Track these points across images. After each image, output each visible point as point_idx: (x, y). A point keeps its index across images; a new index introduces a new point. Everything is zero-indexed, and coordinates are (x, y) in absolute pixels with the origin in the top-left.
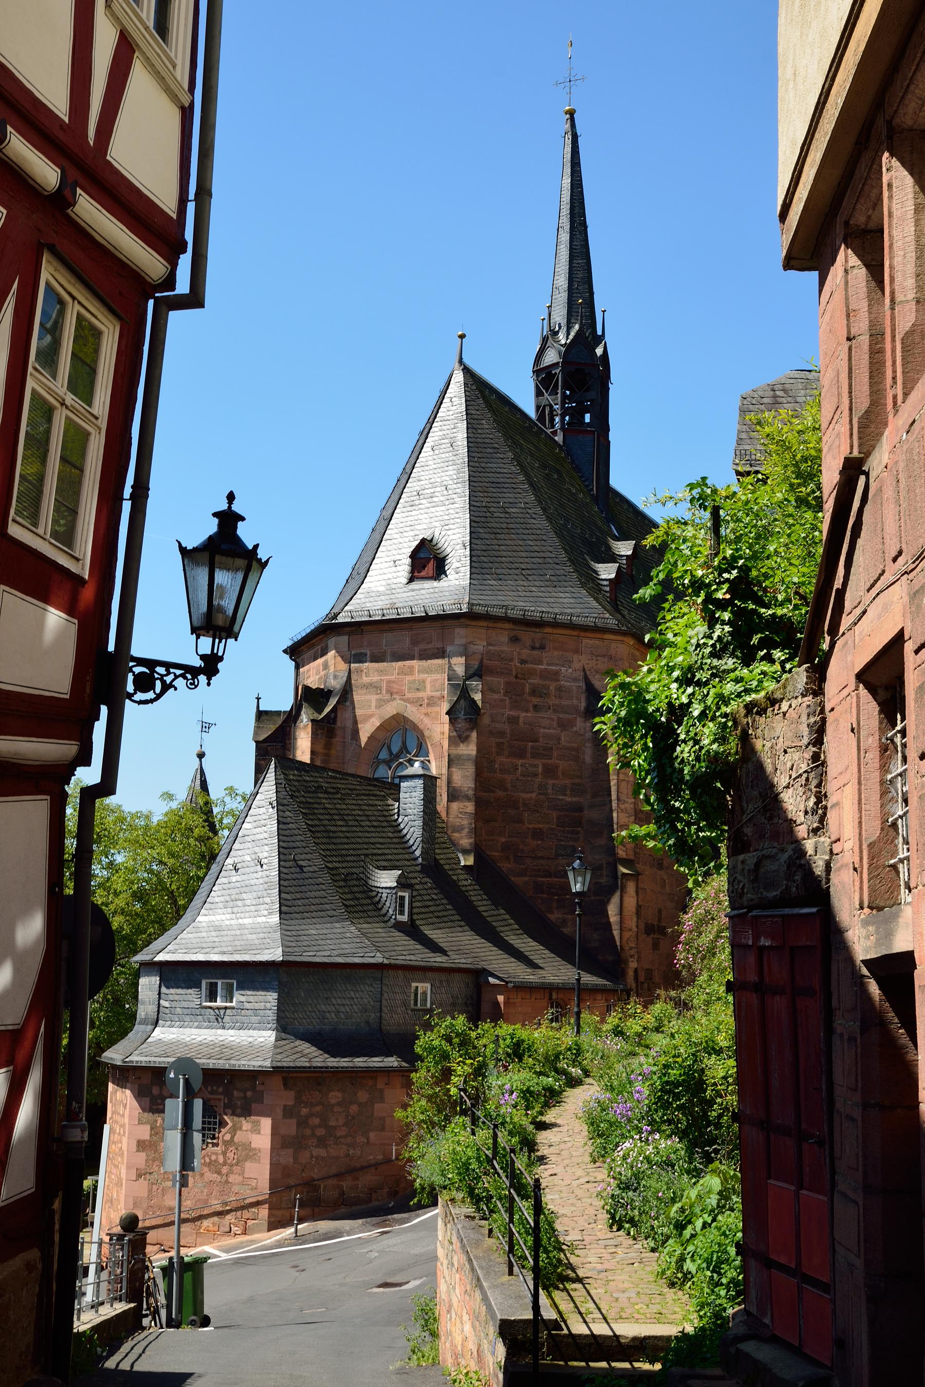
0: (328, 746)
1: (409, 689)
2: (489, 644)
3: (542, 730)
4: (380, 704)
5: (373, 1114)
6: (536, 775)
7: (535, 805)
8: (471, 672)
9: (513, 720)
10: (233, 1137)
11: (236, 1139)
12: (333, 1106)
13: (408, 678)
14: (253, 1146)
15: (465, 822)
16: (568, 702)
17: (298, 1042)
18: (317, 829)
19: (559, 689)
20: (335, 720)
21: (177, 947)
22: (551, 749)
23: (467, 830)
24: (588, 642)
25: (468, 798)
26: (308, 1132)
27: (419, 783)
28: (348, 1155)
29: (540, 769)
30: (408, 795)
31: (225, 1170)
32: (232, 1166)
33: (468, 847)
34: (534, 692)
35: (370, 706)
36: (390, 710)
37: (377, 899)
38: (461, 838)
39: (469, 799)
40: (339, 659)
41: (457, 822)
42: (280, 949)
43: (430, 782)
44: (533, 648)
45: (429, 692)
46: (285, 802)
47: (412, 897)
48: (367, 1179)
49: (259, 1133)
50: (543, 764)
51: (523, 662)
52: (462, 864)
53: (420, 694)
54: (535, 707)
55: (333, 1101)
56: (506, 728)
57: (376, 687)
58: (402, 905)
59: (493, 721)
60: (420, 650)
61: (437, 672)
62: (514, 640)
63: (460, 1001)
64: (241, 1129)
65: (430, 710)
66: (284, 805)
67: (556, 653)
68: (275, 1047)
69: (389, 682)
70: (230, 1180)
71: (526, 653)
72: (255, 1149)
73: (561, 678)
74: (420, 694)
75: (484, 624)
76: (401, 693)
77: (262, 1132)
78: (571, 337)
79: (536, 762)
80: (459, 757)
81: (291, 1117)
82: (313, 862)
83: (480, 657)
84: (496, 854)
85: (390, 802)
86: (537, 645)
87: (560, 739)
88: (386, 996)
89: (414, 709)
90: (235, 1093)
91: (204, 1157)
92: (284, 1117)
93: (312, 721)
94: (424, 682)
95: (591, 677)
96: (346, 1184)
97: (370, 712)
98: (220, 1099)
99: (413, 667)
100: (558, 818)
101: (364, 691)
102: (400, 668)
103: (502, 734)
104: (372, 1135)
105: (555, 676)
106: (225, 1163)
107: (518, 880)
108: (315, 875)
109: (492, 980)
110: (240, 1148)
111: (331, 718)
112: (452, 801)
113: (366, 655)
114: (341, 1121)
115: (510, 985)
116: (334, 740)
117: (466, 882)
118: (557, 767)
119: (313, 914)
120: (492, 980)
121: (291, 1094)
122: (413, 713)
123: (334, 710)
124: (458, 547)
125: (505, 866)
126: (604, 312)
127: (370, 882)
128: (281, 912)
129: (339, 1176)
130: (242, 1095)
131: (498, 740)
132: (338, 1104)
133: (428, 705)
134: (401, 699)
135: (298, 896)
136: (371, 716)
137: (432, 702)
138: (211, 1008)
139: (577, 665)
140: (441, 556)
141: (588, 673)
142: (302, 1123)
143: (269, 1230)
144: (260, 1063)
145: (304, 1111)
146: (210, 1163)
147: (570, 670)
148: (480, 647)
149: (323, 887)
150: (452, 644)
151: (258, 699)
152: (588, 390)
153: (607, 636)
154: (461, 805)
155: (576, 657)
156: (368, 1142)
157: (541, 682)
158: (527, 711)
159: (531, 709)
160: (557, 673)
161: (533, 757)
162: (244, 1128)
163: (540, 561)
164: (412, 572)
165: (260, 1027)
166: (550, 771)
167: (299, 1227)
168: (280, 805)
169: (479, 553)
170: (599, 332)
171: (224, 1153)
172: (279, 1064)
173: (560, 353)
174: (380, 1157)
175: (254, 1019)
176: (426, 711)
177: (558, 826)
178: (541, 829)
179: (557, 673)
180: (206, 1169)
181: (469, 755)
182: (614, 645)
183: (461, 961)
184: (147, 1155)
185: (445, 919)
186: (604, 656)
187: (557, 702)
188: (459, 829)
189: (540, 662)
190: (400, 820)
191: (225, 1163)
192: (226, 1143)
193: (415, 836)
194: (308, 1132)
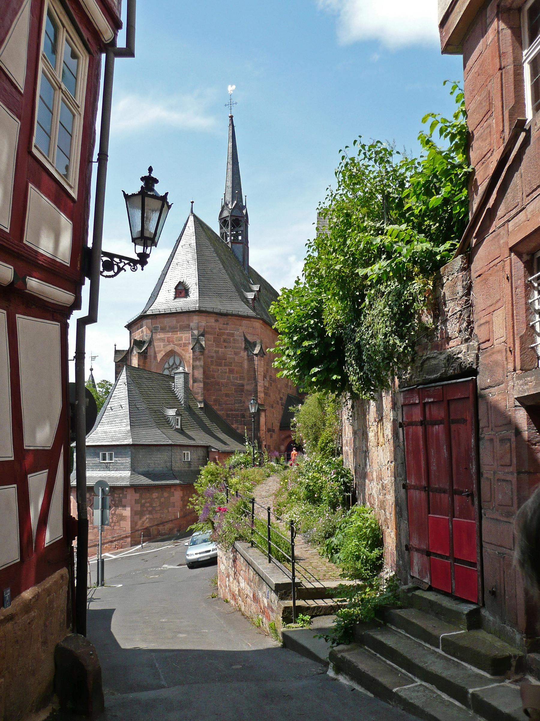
0: (145, 363)
4: (165, 346)
6: (226, 373)
8: (200, 333)
9: (217, 352)
10: (115, 512)
11: (116, 513)
12: (155, 499)
15: (200, 391)
16: (238, 345)
17: (140, 475)
18: (144, 393)
19: (234, 340)
20: (147, 353)
21: (89, 440)
22: (231, 363)
23: (200, 394)
24: (245, 322)
25: (200, 381)
26: (145, 509)
27: (182, 375)
28: (160, 517)
30: (178, 380)
31: (112, 525)
32: (115, 523)
33: (201, 400)
34: (225, 341)
35: (161, 347)
36: (169, 348)
37: (168, 420)
38: (198, 397)
39: (201, 382)
40: (147, 329)
41: (197, 391)
42: (131, 439)
43: (186, 374)
44: (224, 324)
46: (130, 383)
47: (181, 419)
48: (168, 526)
50: (229, 369)
51: (220, 329)
52: (199, 407)
53: (181, 342)
54: (225, 347)
55: (154, 497)
56: (214, 355)
58: (178, 422)
62: (217, 321)
63: (201, 458)
65: (184, 348)
66: (130, 384)
67: (232, 326)
68: (131, 477)
69: (169, 337)
71: (221, 325)
72: (124, 516)
73: (235, 336)
74: (181, 342)
75: (205, 314)
76: (173, 342)
78: (233, 206)
79: (226, 368)
80: (197, 366)
81: (138, 503)
82: (142, 406)
83: (203, 327)
85: (171, 383)
86: (226, 323)
87: (235, 359)
88: (173, 456)
89: (178, 348)
92: (135, 503)
93: (138, 353)
94: (182, 337)
96: (161, 528)
97: (161, 349)
100: (235, 389)
103: (212, 357)
104: (170, 509)
105: (232, 335)
107: (220, 413)
108: (143, 411)
109: (213, 450)
111: (145, 352)
114: (158, 504)
115: (220, 451)
116: (146, 360)
117: (201, 414)
118: (234, 369)
119: (143, 426)
120: (213, 450)
121: (138, 495)
122: (177, 349)
123: (146, 348)
124: (193, 285)
125: (215, 408)
126: (246, 196)
127: (165, 413)
128: (131, 425)
129: (158, 525)
131: (211, 359)
132: (157, 498)
135: (137, 419)
136: (161, 351)
137: (185, 345)
138: (104, 463)
139: (241, 331)
140: (187, 288)
142: (143, 506)
143: (131, 546)
144: (125, 484)
145: (143, 501)
148: (203, 324)
149: (147, 415)
150: (193, 322)
151: (115, 345)
152: (240, 227)
153: (252, 320)
154: (198, 384)
156: (168, 511)
157: (228, 337)
158: (222, 348)
160: (233, 334)
163: (226, 291)
164: (176, 295)
165: (124, 469)
167: (143, 545)
168: (129, 384)
169: (202, 287)
170: (244, 205)
172: (133, 484)
173: (229, 212)
174: (173, 517)
175: (122, 467)
176: (183, 349)
178: (228, 393)
179: (233, 334)
182: (255, 323)
183: (201, 443)
185: (194, 427)
186: (251, 327)
190: (175, 390)
191: (112, 522)
193: (181, 396)
194: (145, 509)
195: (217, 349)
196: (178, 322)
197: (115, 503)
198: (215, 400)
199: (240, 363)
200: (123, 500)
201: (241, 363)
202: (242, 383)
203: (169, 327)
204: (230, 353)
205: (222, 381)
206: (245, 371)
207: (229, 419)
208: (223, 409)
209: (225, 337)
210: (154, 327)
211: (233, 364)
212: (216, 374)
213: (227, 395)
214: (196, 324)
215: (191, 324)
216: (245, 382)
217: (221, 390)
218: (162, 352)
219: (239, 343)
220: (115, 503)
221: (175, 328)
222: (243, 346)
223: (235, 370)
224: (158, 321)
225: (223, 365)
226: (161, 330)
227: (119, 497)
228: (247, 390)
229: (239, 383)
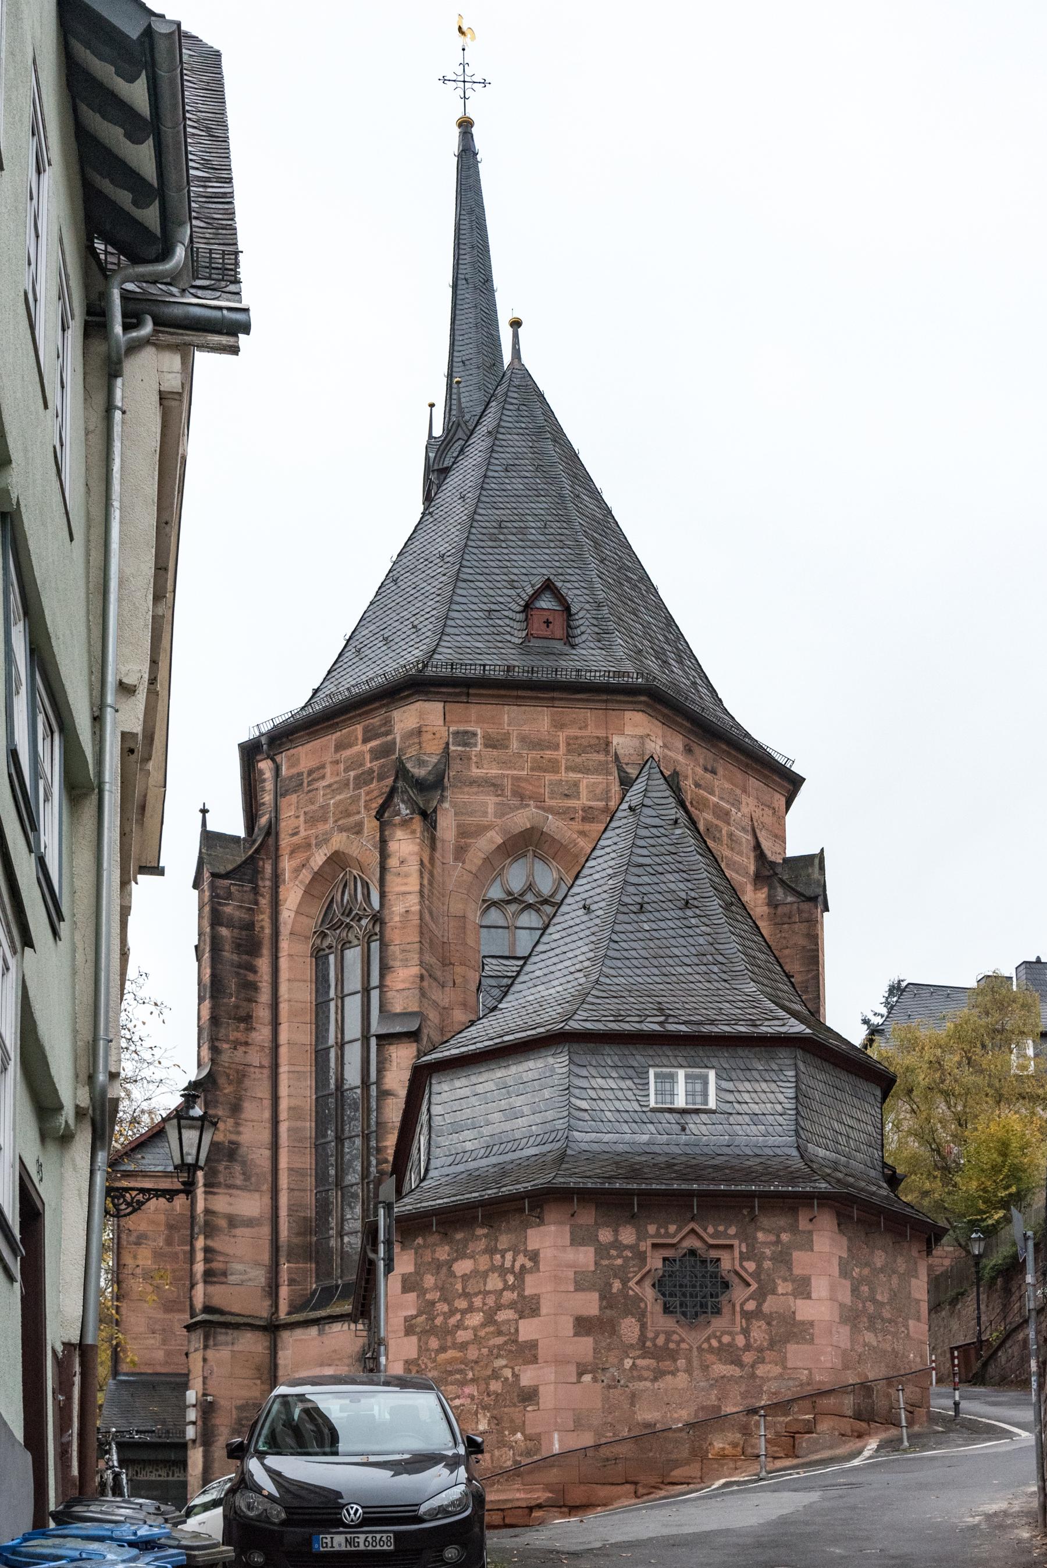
1: (552, 792)
2: (665, 746)
4: (502, 811)
10: (760, 1305)
11: (766, 1308)
13: (549, 777)
14: (798, 1318)
19: (731, 835)
31: (748, 1358)
32: (760, 1350)
36: (522, 819)
45: (584, 800)
49: (809, 1297)
57: (494, 785)
60: (568, 737)
61: (596, 771)
64: (774, 1292)
65: (587, 827)
69: (517, 779)
70: (759, 1373)
71: (699, 771)
72: (803, 1323)
73: (732, 822)
76: (539, 800)
77: (814, 1295)
89: (560, 824)
90: (760, 1236)
91: (708, 1340)
94: (576, 784)
95: (757, 831)
98: (731, 1247)
101: (475, 789)
102: (534, 760)
106: (748, 1347)
110: (774, 1323)
130: (772, 1238)
133: (584, 819)
134: (537, 807)
146: (719, 1349)
151: (204, 811)
162: (780, 1290)
171: (746, 1332)
180: (710, 1358)
184: (596, 1342)
191: (748, 1347)
192: (747, 1316)
197: (759, 1266)
200: (796, 1255)
203: (523, 739)
210: (457, 733)
214: (636, 742)
215: (616, 740)
218: (491, 834)
220: (759, 1266)
221: (549, 748)
222: (752, 868)
224: (474, 710)
226: (486, 746)
227: (778, 1241)
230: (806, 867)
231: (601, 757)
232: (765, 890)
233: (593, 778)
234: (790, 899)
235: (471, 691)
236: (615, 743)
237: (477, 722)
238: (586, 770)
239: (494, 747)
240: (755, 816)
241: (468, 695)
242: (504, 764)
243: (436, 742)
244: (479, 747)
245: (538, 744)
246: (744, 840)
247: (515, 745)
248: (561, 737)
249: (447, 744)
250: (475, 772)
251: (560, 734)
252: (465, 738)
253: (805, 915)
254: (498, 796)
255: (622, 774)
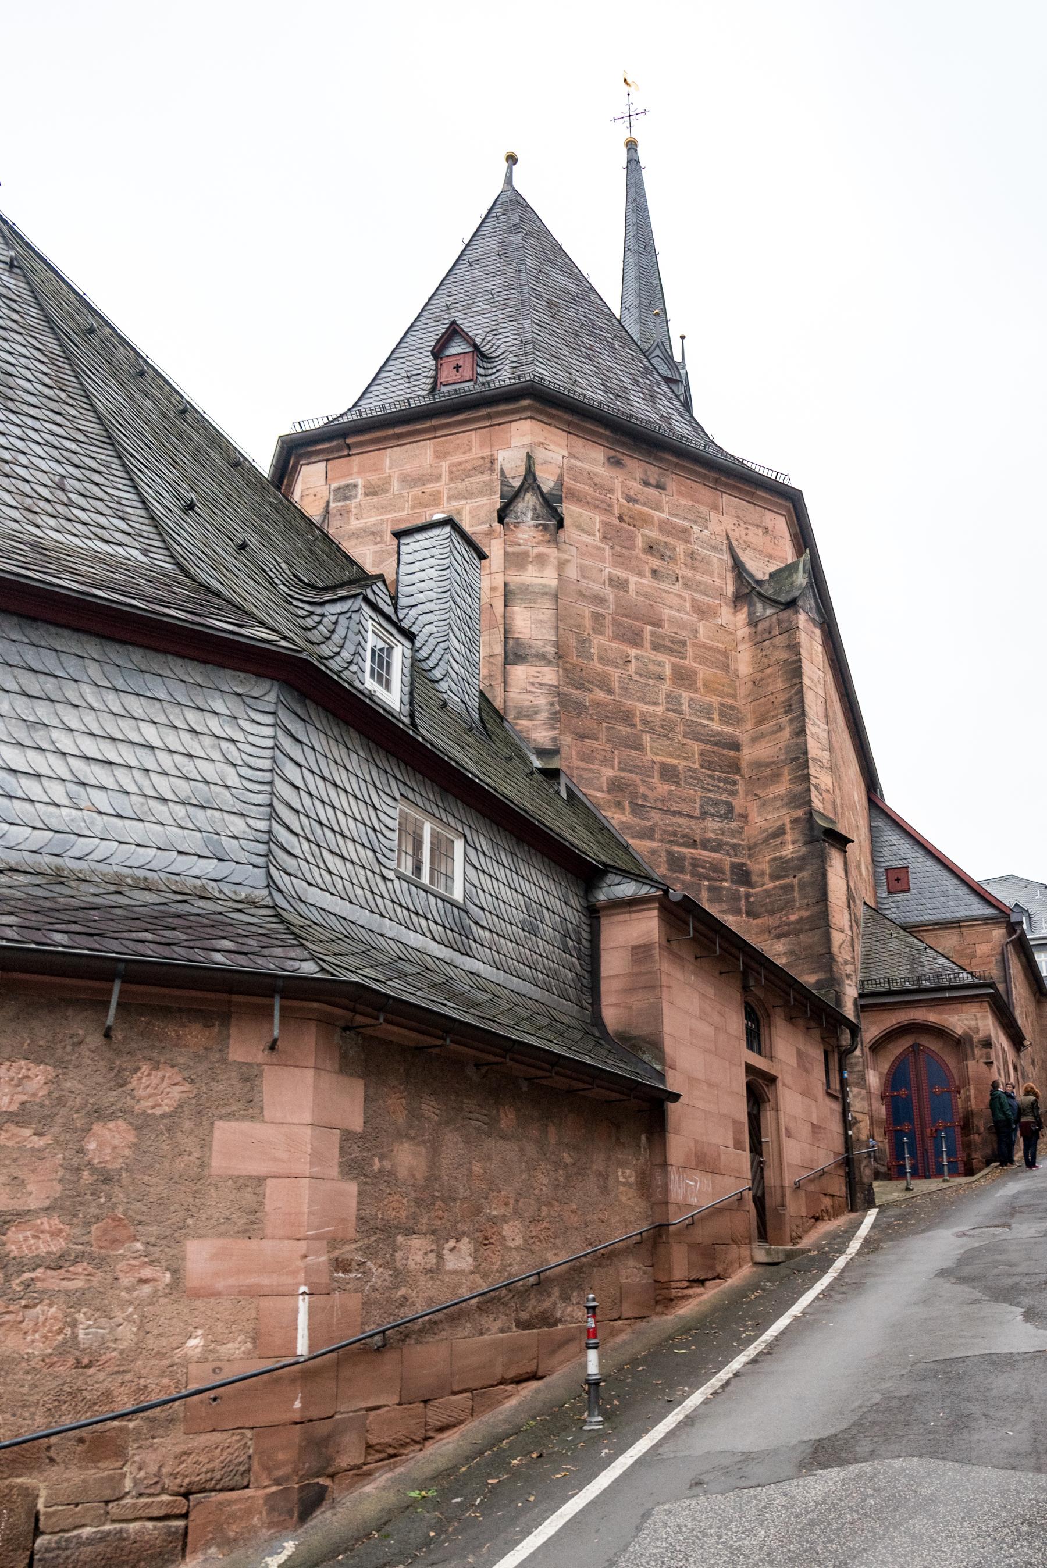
2: (572, 455)
3: (667, 611)
5: (203, 1165)
6: (661, 678)
7: (662, 726)
9: (620, 585)
15: (542, 701)
16: (705, 579)
19: (692, 555)
22: (683, 643)
29: (668, 671)
38: (536, 728)
50: (674, 666)
51: (630, 499)
54: (654, 572)
56: (609, 593)
57: (373, 533)
59: (584, 577)
61: (481, 493)
73: (692, 539)
79: (660, 657)
80: (525, 589)
83: (558, 471)
84: (599, 794)
87: (696, 631)
95: (739, 552)
99: (439, 492)
100: (701, 754)
102: (415, 498)
103: (600, 600)
105: (684, 534)
112: (514, 664)
113: (355, 486)
118: (695, 673)
131: (594, 609)
141: (735, 543)
147: (706, 532)
155: (713, 515)
158: (640, 574)
159: (648, 574)
161: (656, 647)
166: (683, 677)
177: (702, 766)
181: (545, 586)
186: (758, 526)
187: (689, 573)
188: (530, 713)
189: (659, 508)
195: (617, 572)
196: (440, 455)
198: (616, 786)
199: (717, 651)
201: (725, 654)
202: (732, 736)
203: (404, 479)
204: (675, 601)
205: (642, 707)
206: (743, 691)
207: (683, 882)
208: (652, 830)
209: (654, 534)
211: (690, 652)
212: (615, 675)
213: (668, 773)
216: (743, 733)
217: (638, 747)
219: (710, 574)
221: (430, 481)
222: (730, 589)
223: (701, 676)
225: (647, 644)
226: (366, 494)
228: (758, 765)
229: (719, 734)
230: (790, 575)
231: (486, 477)
232: (745, 609)
233: (476, 502)
234: (769, 611)
235: (348, 441)
236: (500, 459)
237: (359, 473)
238: (467, 495)
239: (374, 493)
240: (731, 534)
241: (349, 447)
242: (383, 509)
243: (317, 503)
244: (360, 497)
245: (420, 480)
246: (715, 560)
247: (395, 486)
248: (445, 466)
249: (328, 502)
250: (355, 524)
251: (443, 463)
252: (344, 493)
253: (785, 625)
254: (376, 544)
255: (506, 489)
